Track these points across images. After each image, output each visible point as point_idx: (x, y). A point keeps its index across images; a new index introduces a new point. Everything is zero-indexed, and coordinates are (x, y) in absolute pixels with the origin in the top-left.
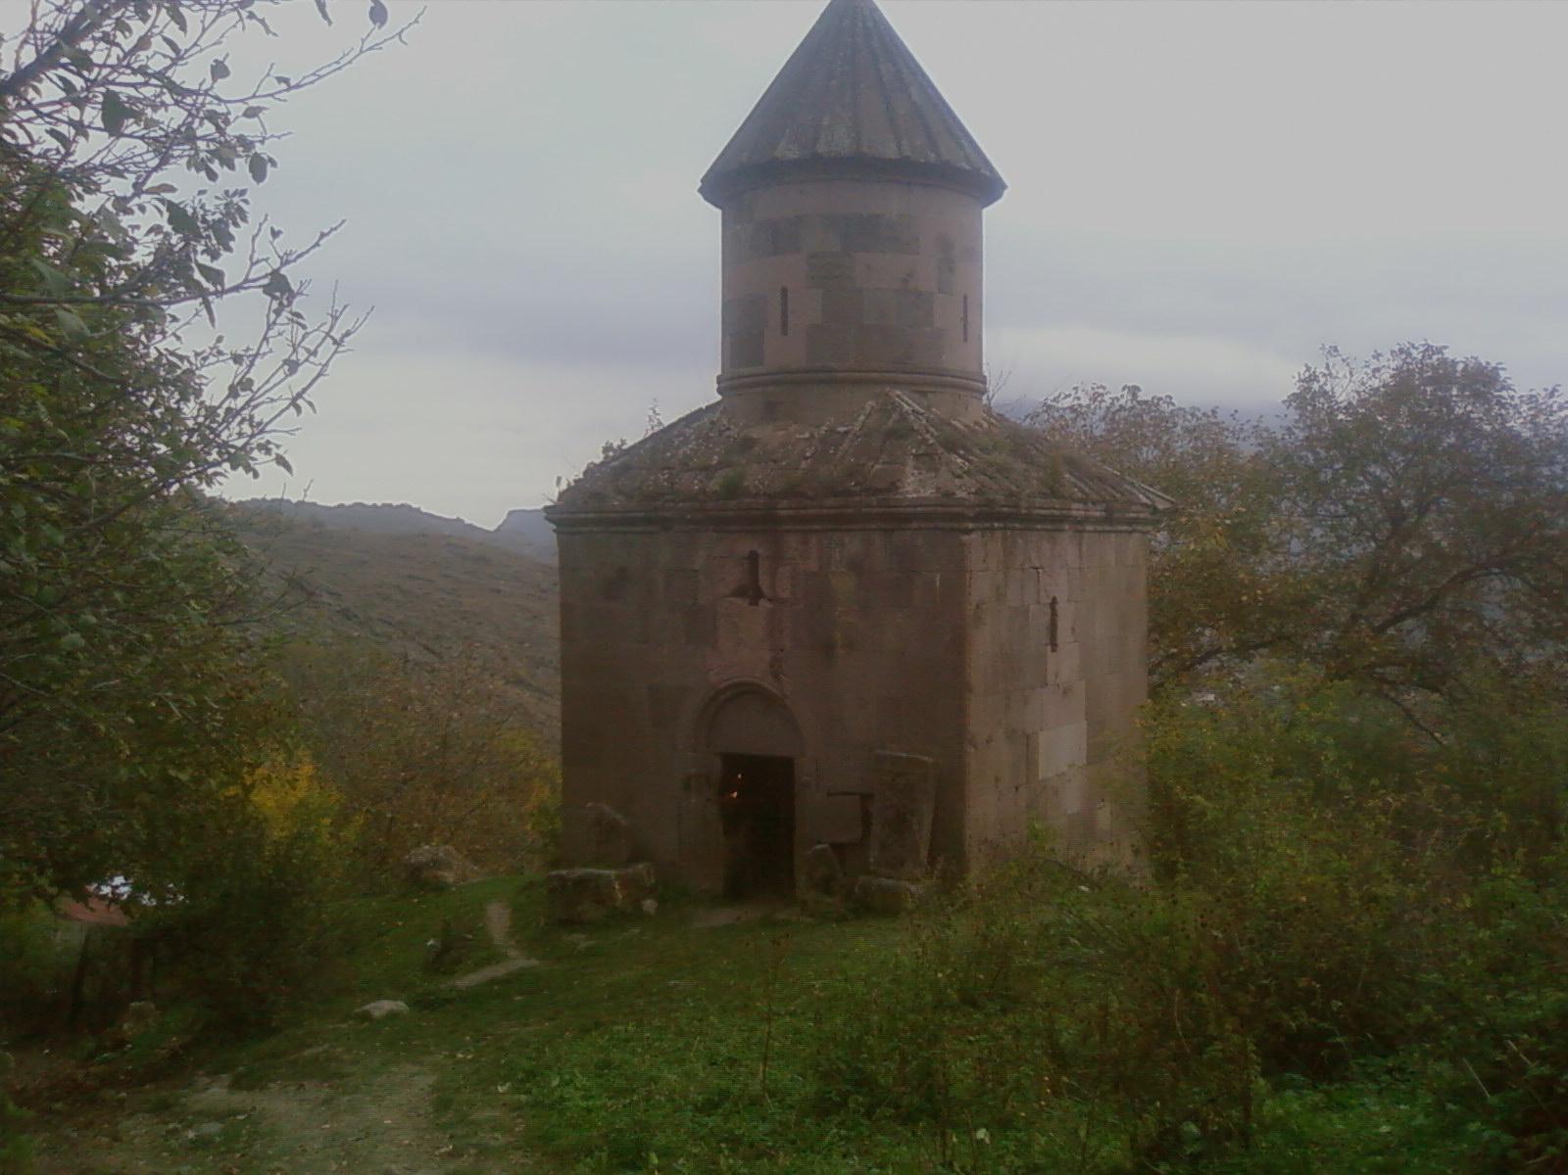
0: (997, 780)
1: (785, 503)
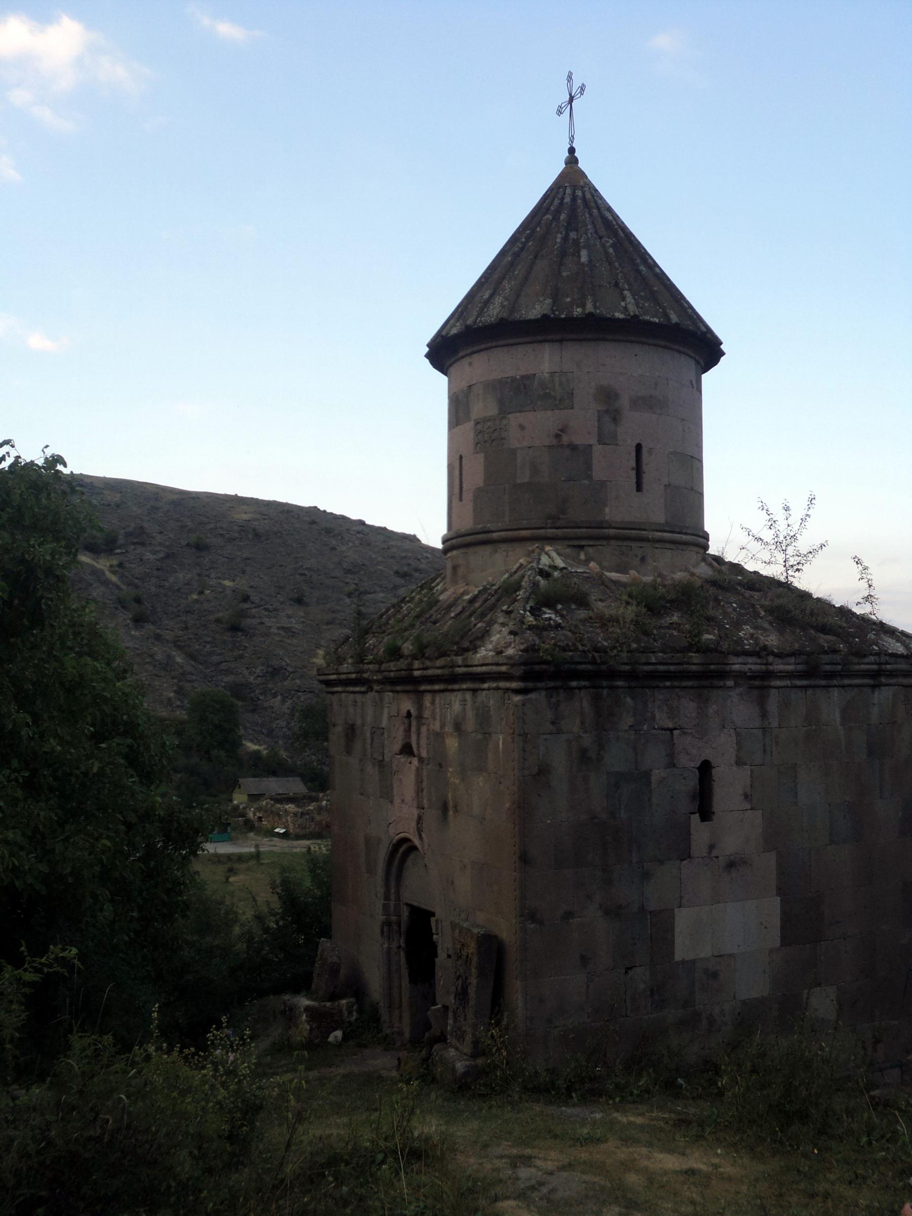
0: (584, 960)
1: (416, 664)
